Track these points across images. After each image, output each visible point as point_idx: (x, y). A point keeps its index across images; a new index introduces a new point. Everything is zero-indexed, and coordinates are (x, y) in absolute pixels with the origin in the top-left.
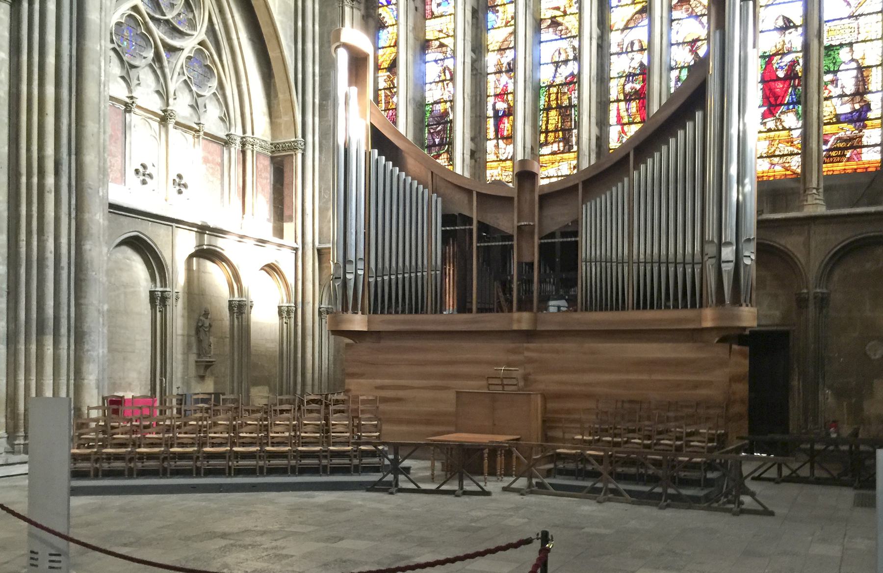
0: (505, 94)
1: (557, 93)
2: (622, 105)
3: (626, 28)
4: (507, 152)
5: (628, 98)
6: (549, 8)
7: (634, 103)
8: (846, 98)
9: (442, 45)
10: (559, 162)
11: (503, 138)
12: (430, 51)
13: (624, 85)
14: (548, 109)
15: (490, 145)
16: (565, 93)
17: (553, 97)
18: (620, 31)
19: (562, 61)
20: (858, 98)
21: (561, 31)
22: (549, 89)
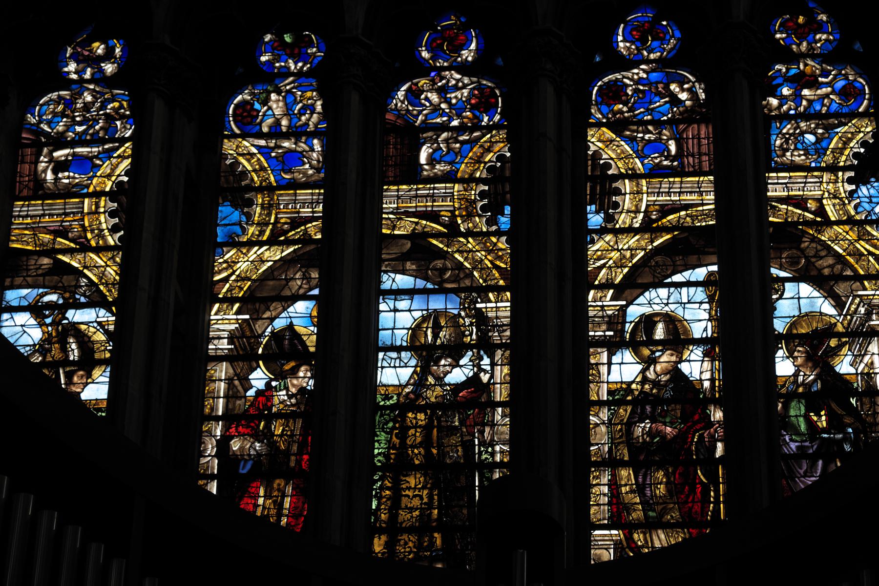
0: (260, 417)
1: (427, 429)
7: (661, 473)
13: (630, 425)
17: (415, 436)
22: (403, 416)
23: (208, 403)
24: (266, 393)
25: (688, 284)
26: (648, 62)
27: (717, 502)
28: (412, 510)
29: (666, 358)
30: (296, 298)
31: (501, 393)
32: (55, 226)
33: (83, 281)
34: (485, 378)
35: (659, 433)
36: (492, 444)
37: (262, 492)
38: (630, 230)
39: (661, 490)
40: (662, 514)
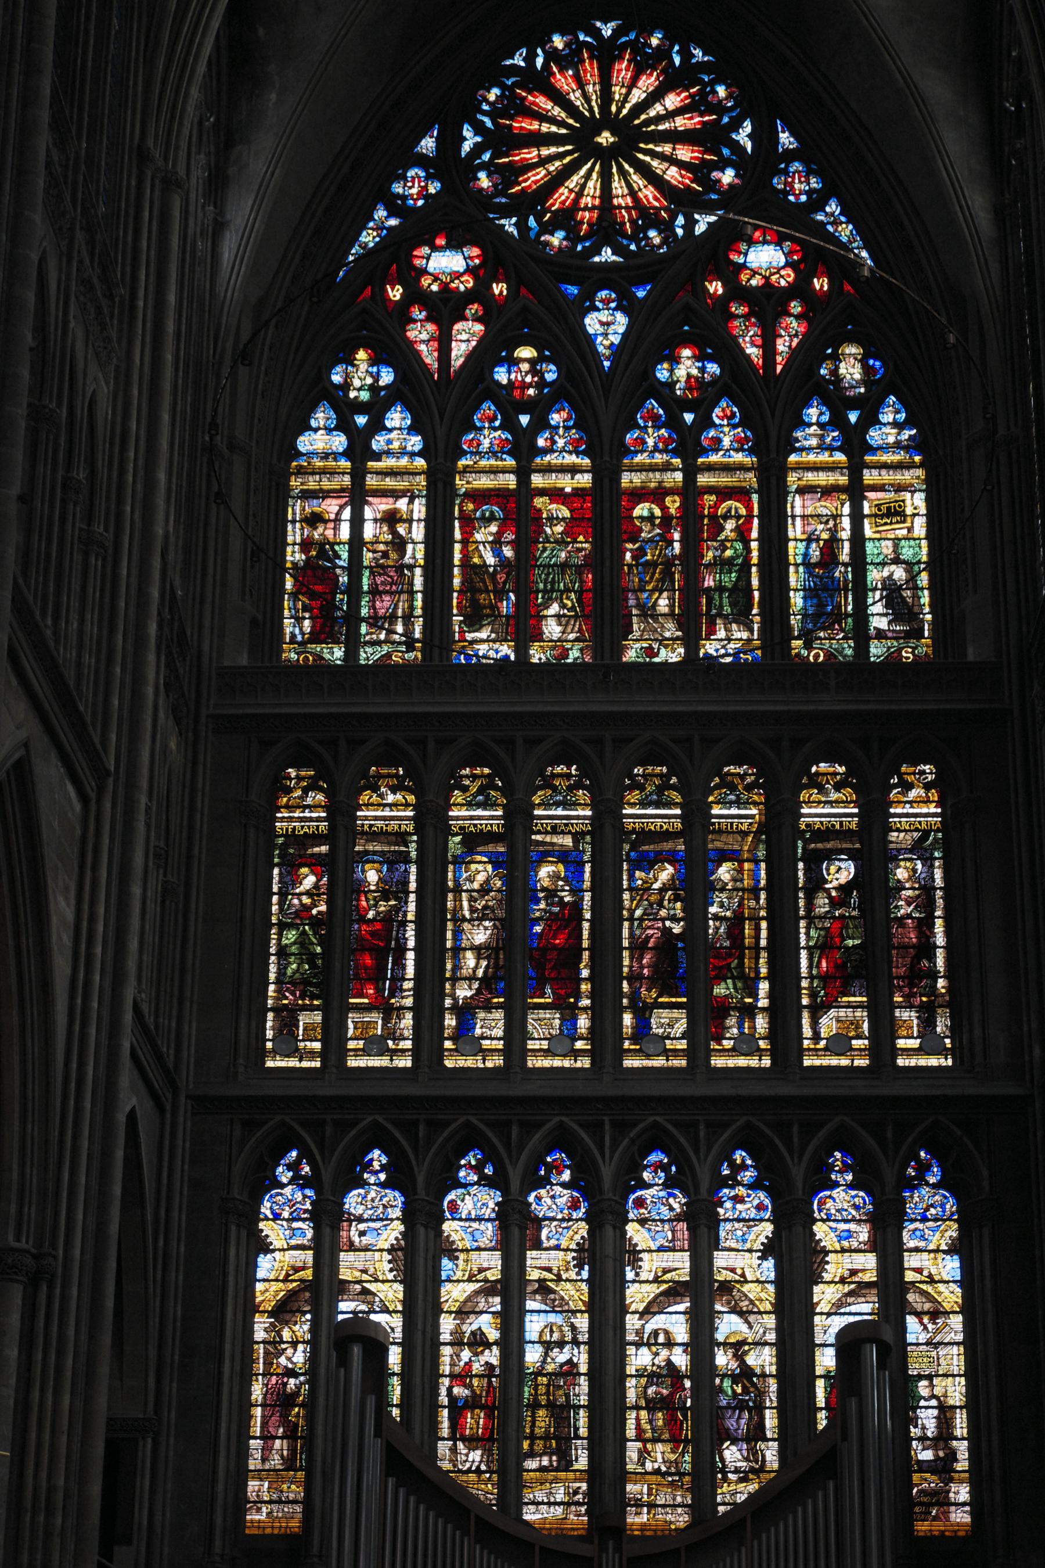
0: (467, 1376)
1: (548, 1385)
2: (644, 1414)
3: (647, 1313)
4: (470, 1459)
5: (652, 1405)
6: (535, 1267)
8: (928, 1442)
9: (365, 1292)
10: (551, 1483)
11: (463, 1439)
12: (345, 1297)
13: (646, 1388)
14: (535, 1405)
15: (443, 1448)
16: (560, 1387)
17: (542, 1390)
18: (637, 1316)
19: (554, 1342)
20: (942, 1444)
21: (554, 1300)
23: (441, 1367)
24: (469, 1364)
25: (676, 1313)
26: (658, 1185)
27: (687, 1430)
28: (541, 1428)
29: (664, 1353)
30: (481, 1312)
31: (583, 1368)
32: (361, 1267)
33: (377, 1299)
34: (575, 1360)
35: (660, 1393)
36: (578, 1395)
37: (469, 1415)
38: (647, 1282)
39: (660, 1423)
40: (660, 1435)
